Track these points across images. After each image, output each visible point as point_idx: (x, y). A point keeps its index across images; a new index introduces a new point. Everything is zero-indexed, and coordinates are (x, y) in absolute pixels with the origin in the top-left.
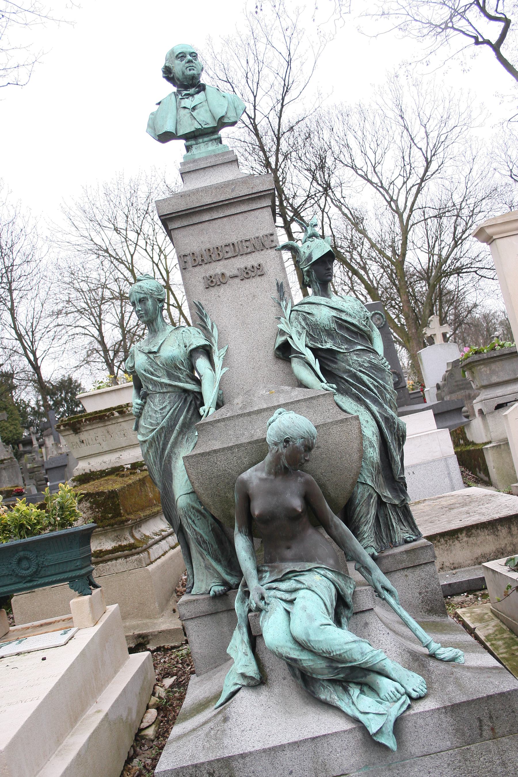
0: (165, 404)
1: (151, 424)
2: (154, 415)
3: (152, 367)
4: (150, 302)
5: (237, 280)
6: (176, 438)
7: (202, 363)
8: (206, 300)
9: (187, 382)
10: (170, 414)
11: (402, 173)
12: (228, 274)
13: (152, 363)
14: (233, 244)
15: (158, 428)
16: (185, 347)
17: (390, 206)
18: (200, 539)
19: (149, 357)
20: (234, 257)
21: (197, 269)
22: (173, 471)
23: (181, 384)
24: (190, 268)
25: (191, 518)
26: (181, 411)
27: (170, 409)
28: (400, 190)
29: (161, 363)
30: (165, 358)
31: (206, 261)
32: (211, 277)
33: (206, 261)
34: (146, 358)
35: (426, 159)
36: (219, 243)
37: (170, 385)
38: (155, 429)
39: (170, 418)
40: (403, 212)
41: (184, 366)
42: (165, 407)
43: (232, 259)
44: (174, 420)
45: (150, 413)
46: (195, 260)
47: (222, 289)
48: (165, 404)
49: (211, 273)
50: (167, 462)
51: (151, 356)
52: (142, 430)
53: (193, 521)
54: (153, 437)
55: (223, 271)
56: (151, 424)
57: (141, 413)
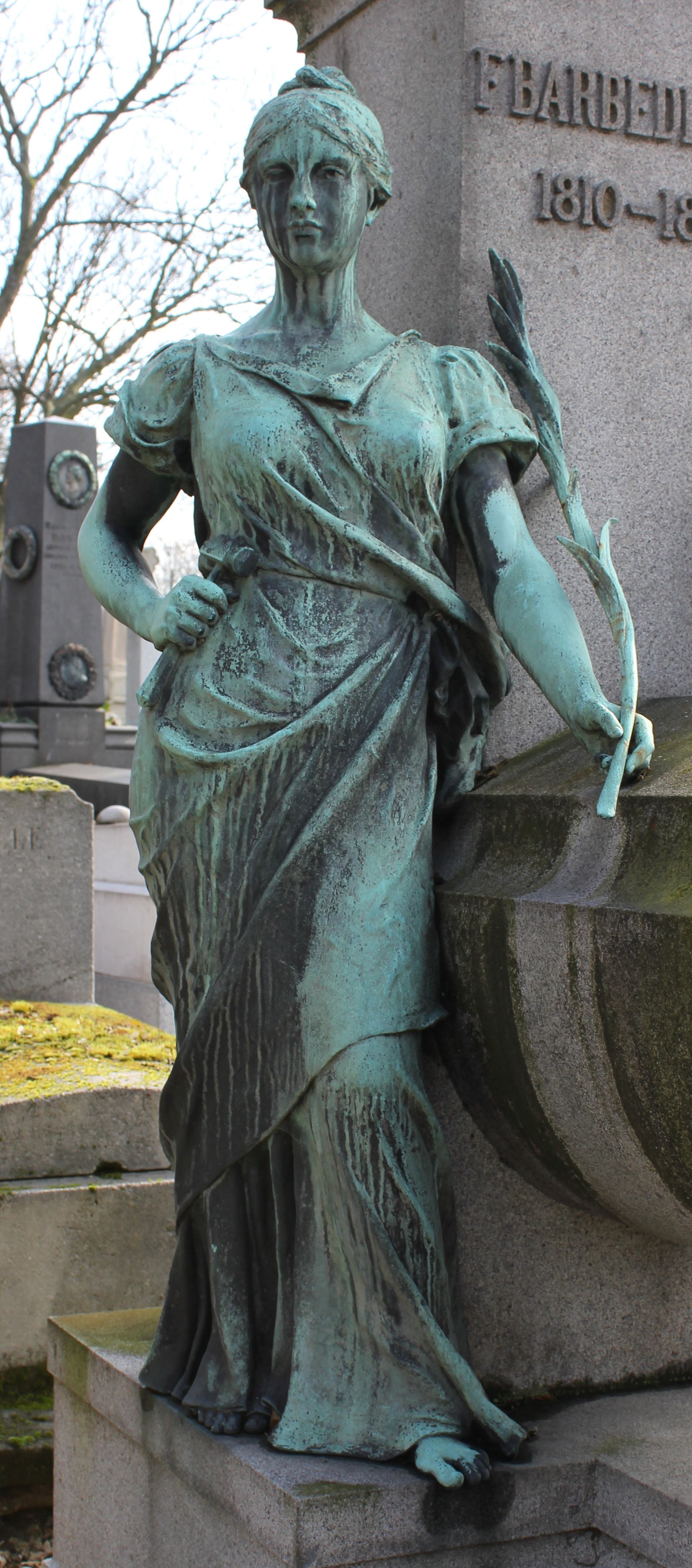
1: (259, 701)
2: (282, 664)
3: (315, 461)
5: (646, 233)
6: (361, 787)
7: (503, 510)
10: (356, 679)
11: (62, 65)
12: (625, 198)
13: (323, 442)
14: (669, 93)
15: (299, 724)
16: (453, 423)
17: (8, 146)
18: (407, 1233)
19: (309, 418)
20: (661, 141)
21: (524, 131)
22: (321, 923)
24: (499, 119)
25: (392, 1141)
26: (395, 681)
27: (358, 662)
28: (43, 109)
29: (364, 456)
30: (389, 444)
32: (568, 184)
33: (564, 117)
34: (298, 415)
35: (154, 51)
36: (617, 66)
37: (379, 562)
39: (355, 700)
40: (38, 178)
42: (339, 647)
43: (650, 147)
44: (365, 712)
45: (265, 653)
47: (594, 245)
49: (570, 168)
50: (297, 875)
51: (324, 415)
52: (192, 713)
53: (398, 1155)
54: (262, 759)
55: (612, 179)
56: (259, 701)
57: (201, 639)
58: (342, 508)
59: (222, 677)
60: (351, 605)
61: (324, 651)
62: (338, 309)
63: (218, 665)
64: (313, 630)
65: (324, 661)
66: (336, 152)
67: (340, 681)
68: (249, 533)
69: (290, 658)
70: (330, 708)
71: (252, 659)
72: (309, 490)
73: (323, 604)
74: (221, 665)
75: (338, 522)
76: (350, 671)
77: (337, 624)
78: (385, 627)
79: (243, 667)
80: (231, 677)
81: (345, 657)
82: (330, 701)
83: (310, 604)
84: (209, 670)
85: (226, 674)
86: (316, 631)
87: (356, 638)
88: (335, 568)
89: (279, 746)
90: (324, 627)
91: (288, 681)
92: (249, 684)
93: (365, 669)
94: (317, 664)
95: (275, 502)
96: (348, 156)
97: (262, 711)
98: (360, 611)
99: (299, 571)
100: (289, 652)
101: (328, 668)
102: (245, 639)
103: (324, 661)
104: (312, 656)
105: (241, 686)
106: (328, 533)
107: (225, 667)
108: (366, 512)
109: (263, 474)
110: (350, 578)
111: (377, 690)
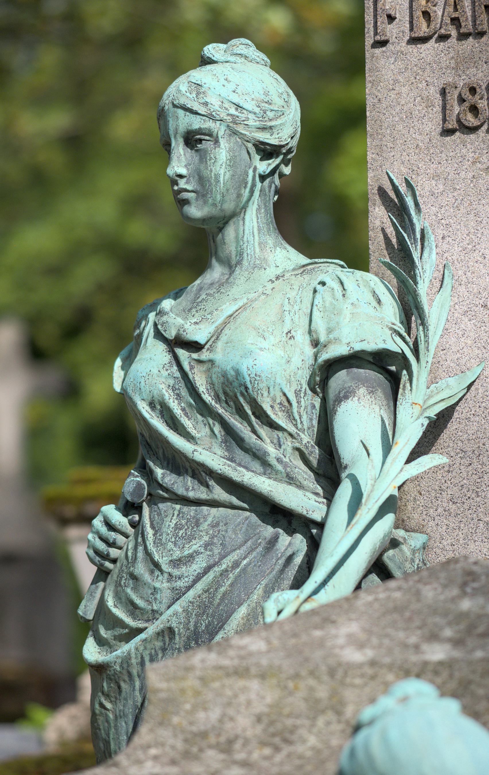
4: (222, 154)
7: (359, 419)
8: (436, 176)
9: (290, 479)
15: (152, 629)
16: (315, 343)
23: (263, 484)
31: (467, 26)
32: (473, 90)
33: (467, 26)
38: (140, 631)
41: (290, 417)
42: (191, 558)
46: (426, 14)
48: (196, 545)
58: (198, 435)
60: (205, 521)
61: (176, 563)
62: (240, 254)
65: (176, 572)
66: (197, 123)
67: (188, 588)
69: (152, 572)
70: (175, 614)
76: (198, 578)
77: (190, 538)
81: (194, 567)
82: (177, 607)
86: (172, 546)
87: (206, 549)
88: (193, 489)
89: (137, 649)
91: (150, 592)
93: (210, 576)
94: (170, 575)
96: (209, 124)
97: (134, 619)
101: (180, 578)
108: (219, 436)
111: (224, 594)
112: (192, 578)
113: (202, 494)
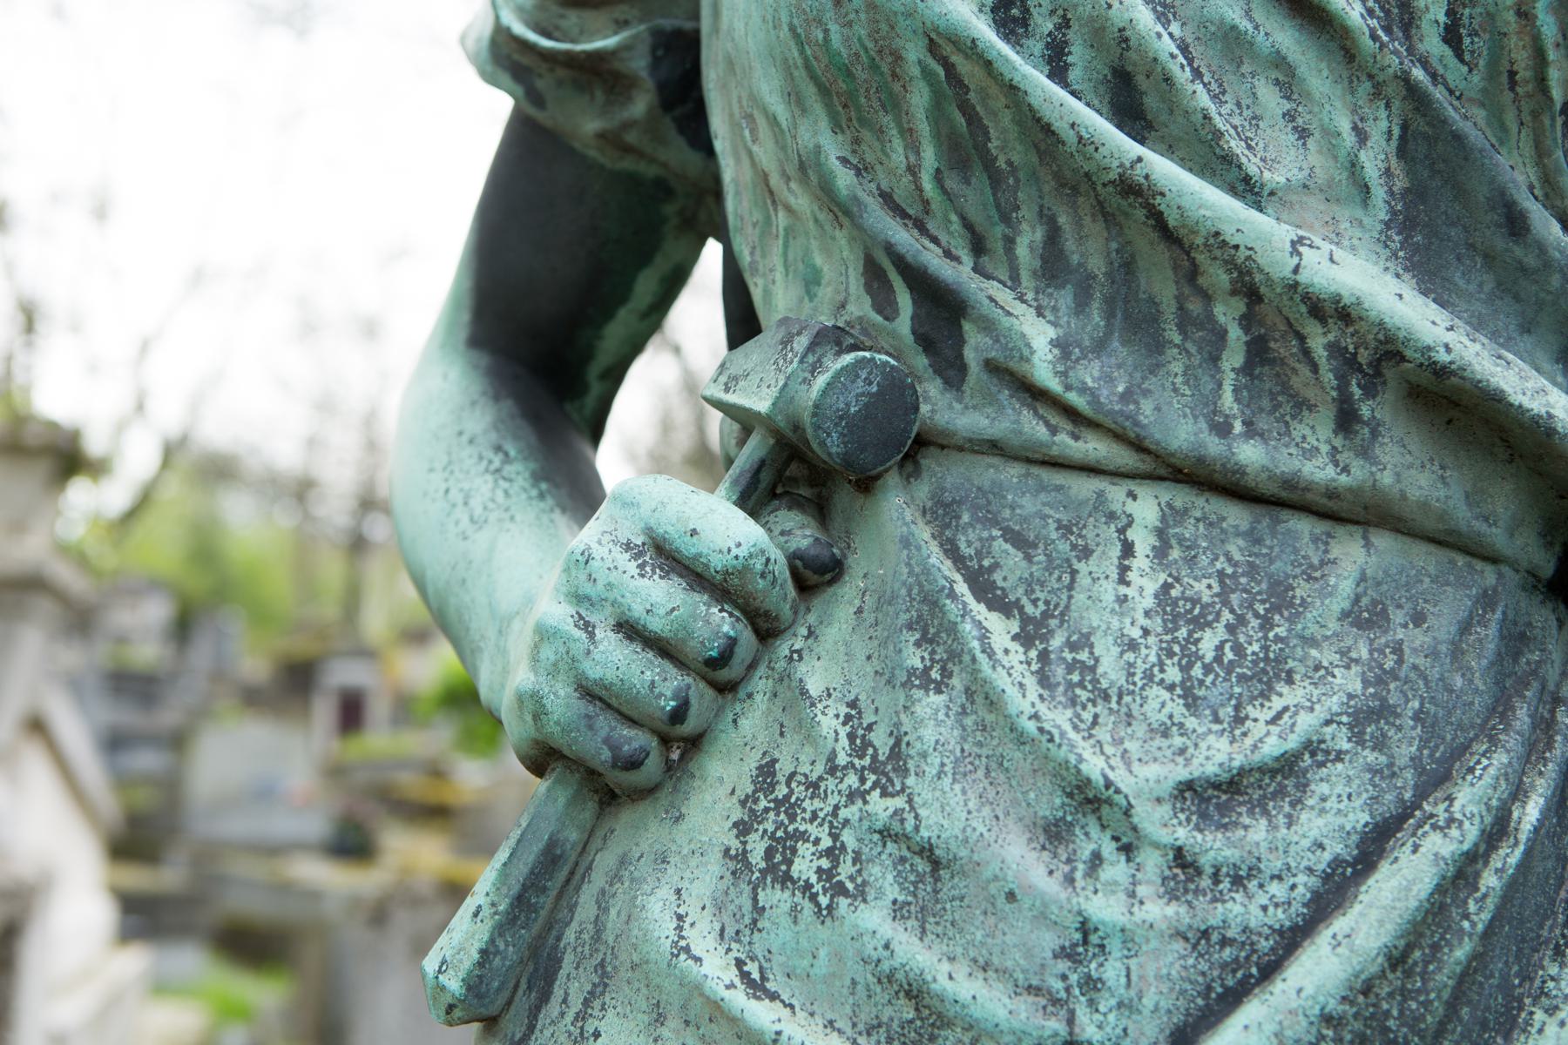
0: (1301, 711)
2: (1020, 859)
27: (1373, 847)
42: (1284, 777)
45: (946, 808)
48: (1301, 711)
57: (682, 741)
58: (1274, 178)
59: (759, 910)
60: (1327, 593)
63: (743, 857)
64: (1160, 704)
65: (1213, 847)
67: (1293, 938)
68: (885, 306)
69: (1054, 834)
71: (886, 834)
72: (1131, 95)
73: (1205, 589)
74: (757, 857)
75: (1264, 234)
76: (1336, 888)
77: (1269, 674)
78: (1473, 681)
79: (846, 869)
80: (795, 911)
81: (1312, 824)
83: (1145, 583)
84: (705, 879)
85: (776, 898)
86: (1177, 708)
87: (1358, 738)
88: (1251, 431)
90: (1214, 691)
91: (1049, 941)
92: (871, 948)
94: (1181, 859)
95: (989, 163)
98: (1366, 615)
99: (1093, 447)
100: (1050, 803)
101: (1238, 881)
102: (860, 745)
103: (1213, 847)
104: (1162, 825)
105: (838, 956)
106: (1218, 277)
107: (771, 869)
108: (1379, 193)
109: (933, 47)
110: (1319, 471)
111: (1465, 977)
112: (1304, 884)
113: (1310, 455)
